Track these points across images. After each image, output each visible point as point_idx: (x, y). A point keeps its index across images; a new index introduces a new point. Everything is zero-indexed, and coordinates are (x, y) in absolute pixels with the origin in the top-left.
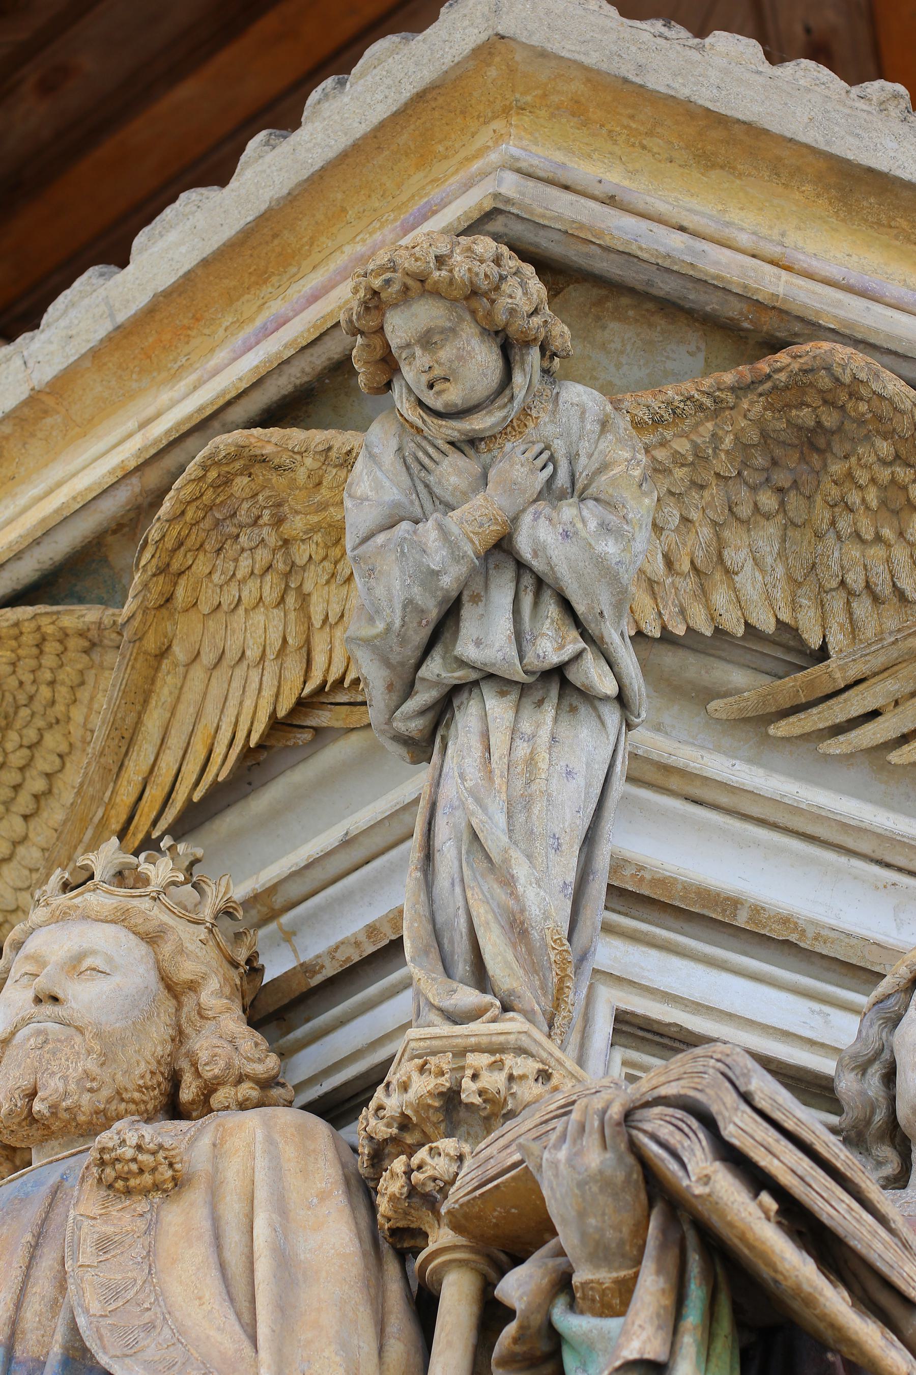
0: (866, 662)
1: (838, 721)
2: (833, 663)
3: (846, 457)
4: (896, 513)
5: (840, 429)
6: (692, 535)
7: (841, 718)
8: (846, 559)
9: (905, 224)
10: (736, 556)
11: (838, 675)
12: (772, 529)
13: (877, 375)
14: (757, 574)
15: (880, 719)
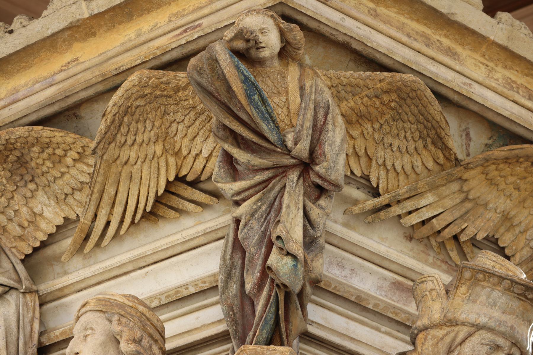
0: (89, 212)
1: (99, 234)
2: (82, 219)
3: (32, 160)
4: (60, 162)
5: (23, 154)
6: (22, 213)
7: (100, 233)
8: (61, 186)
9: (24, 64)
10: (37, 210)
11: (86, 222)
12: (40, 193)
13: (12, 133)
14: (49, 208)
15: (111, 223)
